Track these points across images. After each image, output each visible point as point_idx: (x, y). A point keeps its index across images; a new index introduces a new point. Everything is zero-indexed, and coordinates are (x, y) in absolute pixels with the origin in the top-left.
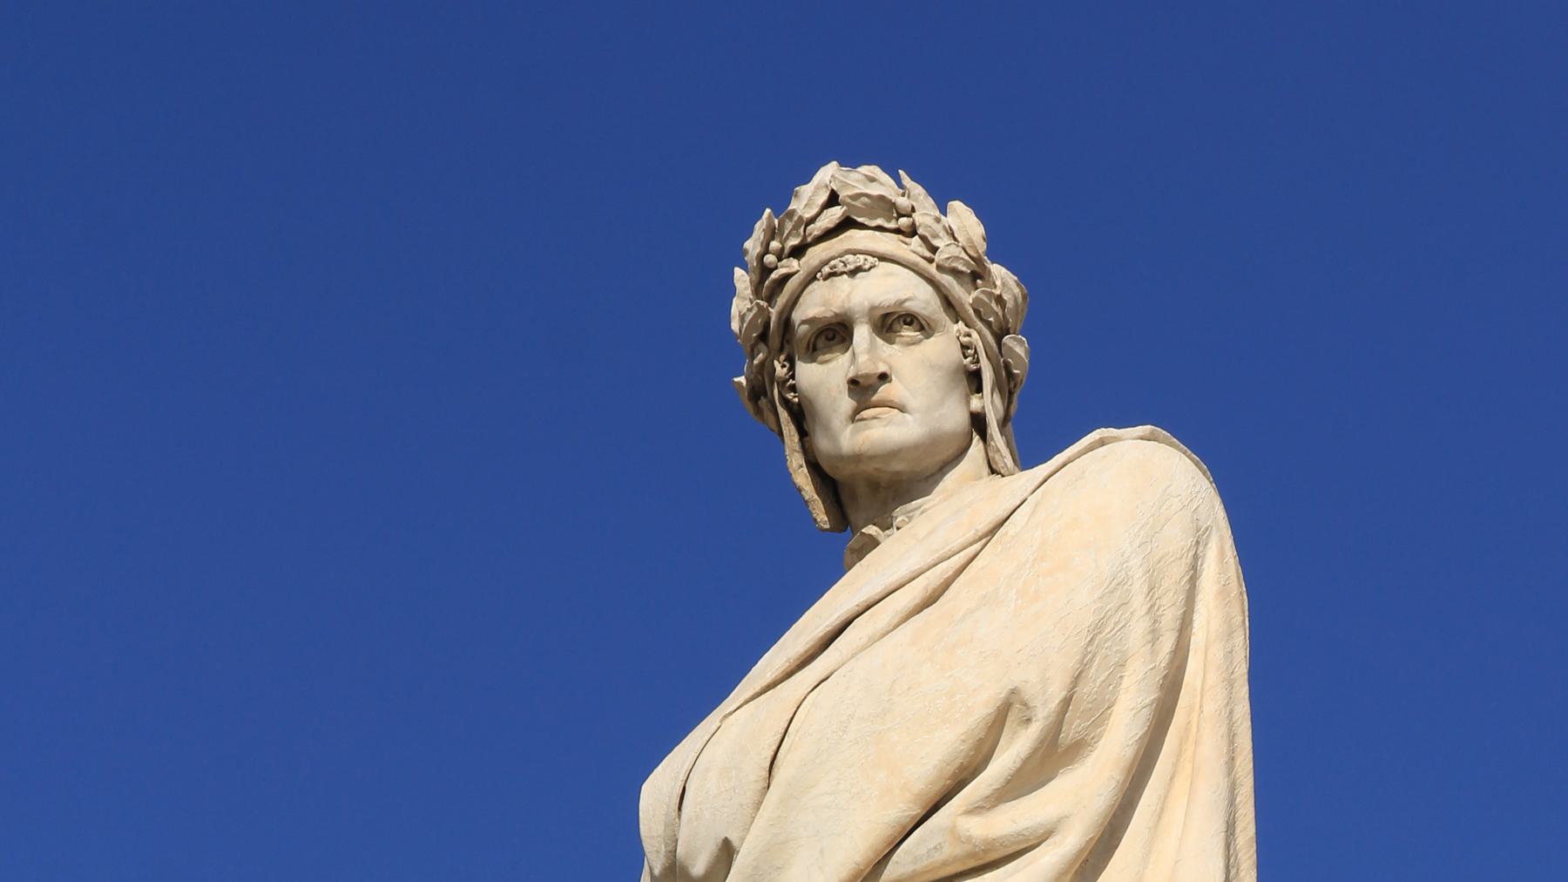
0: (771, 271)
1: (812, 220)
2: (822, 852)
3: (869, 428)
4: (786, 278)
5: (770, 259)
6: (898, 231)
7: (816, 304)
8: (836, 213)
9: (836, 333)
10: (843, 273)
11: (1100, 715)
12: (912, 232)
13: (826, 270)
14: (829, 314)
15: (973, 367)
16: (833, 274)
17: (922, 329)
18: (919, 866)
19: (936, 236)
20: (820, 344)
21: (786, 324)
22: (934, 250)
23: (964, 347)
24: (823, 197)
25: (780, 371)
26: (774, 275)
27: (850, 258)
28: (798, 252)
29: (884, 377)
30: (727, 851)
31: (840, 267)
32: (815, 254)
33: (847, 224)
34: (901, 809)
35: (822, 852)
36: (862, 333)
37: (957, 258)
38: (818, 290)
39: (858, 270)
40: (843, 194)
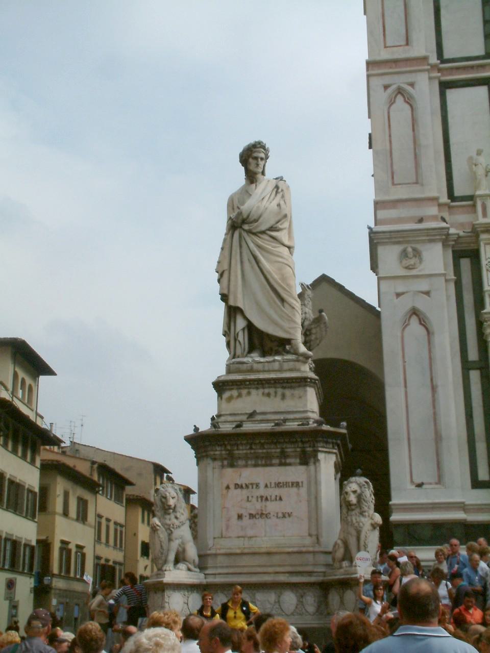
9: (256, 158)
21: (251, 154)
32: (258, 149)
33: (260, 147)
36: (259, 160)
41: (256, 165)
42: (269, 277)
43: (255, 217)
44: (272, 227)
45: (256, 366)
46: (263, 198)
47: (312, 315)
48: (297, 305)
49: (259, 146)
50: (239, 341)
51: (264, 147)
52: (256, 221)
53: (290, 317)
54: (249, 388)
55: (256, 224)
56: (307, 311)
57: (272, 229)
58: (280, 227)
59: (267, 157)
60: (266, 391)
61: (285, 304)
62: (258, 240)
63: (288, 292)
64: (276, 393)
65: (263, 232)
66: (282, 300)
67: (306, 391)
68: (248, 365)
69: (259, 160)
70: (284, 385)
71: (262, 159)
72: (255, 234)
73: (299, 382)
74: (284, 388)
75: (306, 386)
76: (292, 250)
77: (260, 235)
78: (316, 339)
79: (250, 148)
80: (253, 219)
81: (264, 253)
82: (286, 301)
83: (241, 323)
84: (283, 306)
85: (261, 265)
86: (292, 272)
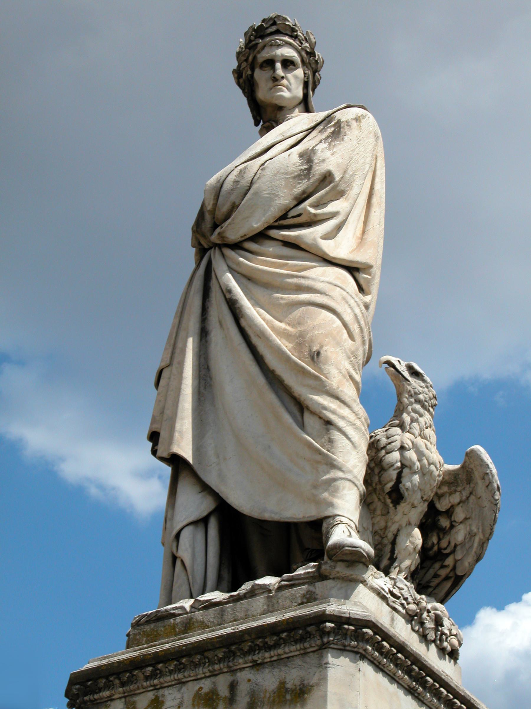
1: (267, 28)
2: (264, 210)
4: (257, 44)
6: (291, 36)
9: (270, 63)
10: (275, 45)
11: (349, 185)
12: (296, 37)
13: (270, 44)
15: (306, 80)
16: (271, 45)
17: (294, 65)
19: (303, 40)
20: (264, 65)
21: (255, 58)
22: (302, 43)
23: (305, 74)
24: (271, 22)
26: (254, 43)
27: (278, 41)
29: (283, 78)
30: (234, 207)
31: (274, 44)
33: (278, 32)
36: (278, 65)
37: (306, 47)
38: (267, 49)
39: (280, 45)
41: (270, 84)
42: (262, 349)
43: (233, 198)
44: (284, 216)
45: (199, 615)
47: (435, 456)
48: (345, 411)
49: (273, 29)
50: (182, 562)
51: (292, 32)
53: (320, 453)
54: (156, 688)
56: (408, 444)
57: (285, 220)
58: (312, 210)
60: (206, 685)
61: (307, 416)
62: (241, 259)
63: (317, 378)
64: (233, 687)
65: (262, 236)
66: (300, 408)
67: (323, 666)
68: (178, 619)
69: (278, 65)
70: (258, 657)
71: (288, 64)
72: (237, 246)
73: (302, 639)
74: (256, 666)
75: (323, 647)
76: (363, 277)
78: (471, 535)
80: (225, 209)
81: (259, 292)
82: (308, 408)
83: (193, 505)
84: (302, 426)
85: (243, 323)
86: (338, 323)
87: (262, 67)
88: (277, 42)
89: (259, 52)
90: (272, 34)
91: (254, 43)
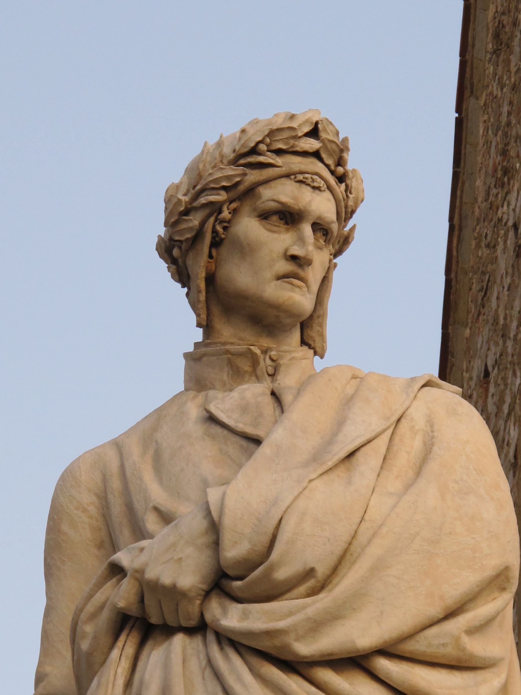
0: (260, 154)
2: (382, 612)
3: (293, 291)
5: (263, 147)
7: (284, 193)
8: (312, 144)
9: (289, 217)
10: (308, 185)
13: (300, 177)
14: (296, 207)
16: (301, 182)
18: (429, 650)
21: (251, 192)
24: (307, 129)
25: (226, 214)
28: (279, 152)
31: (309, 181)
32: (296, 163)
34: (435, 610)
35: (382, 612)
39: (318, 188)
40: (323, 135)
46: (352, 454)
52: (312, 582)
55: (323, 601)
59: (335, 238)
69: (307, 229)
77: (327, 676)
79: (254, 151)
80: (282, 574)
87: (264, 216)
88: (313, 181)
89: (266, 182)
90: (305, 154)
91: (261, 159)
